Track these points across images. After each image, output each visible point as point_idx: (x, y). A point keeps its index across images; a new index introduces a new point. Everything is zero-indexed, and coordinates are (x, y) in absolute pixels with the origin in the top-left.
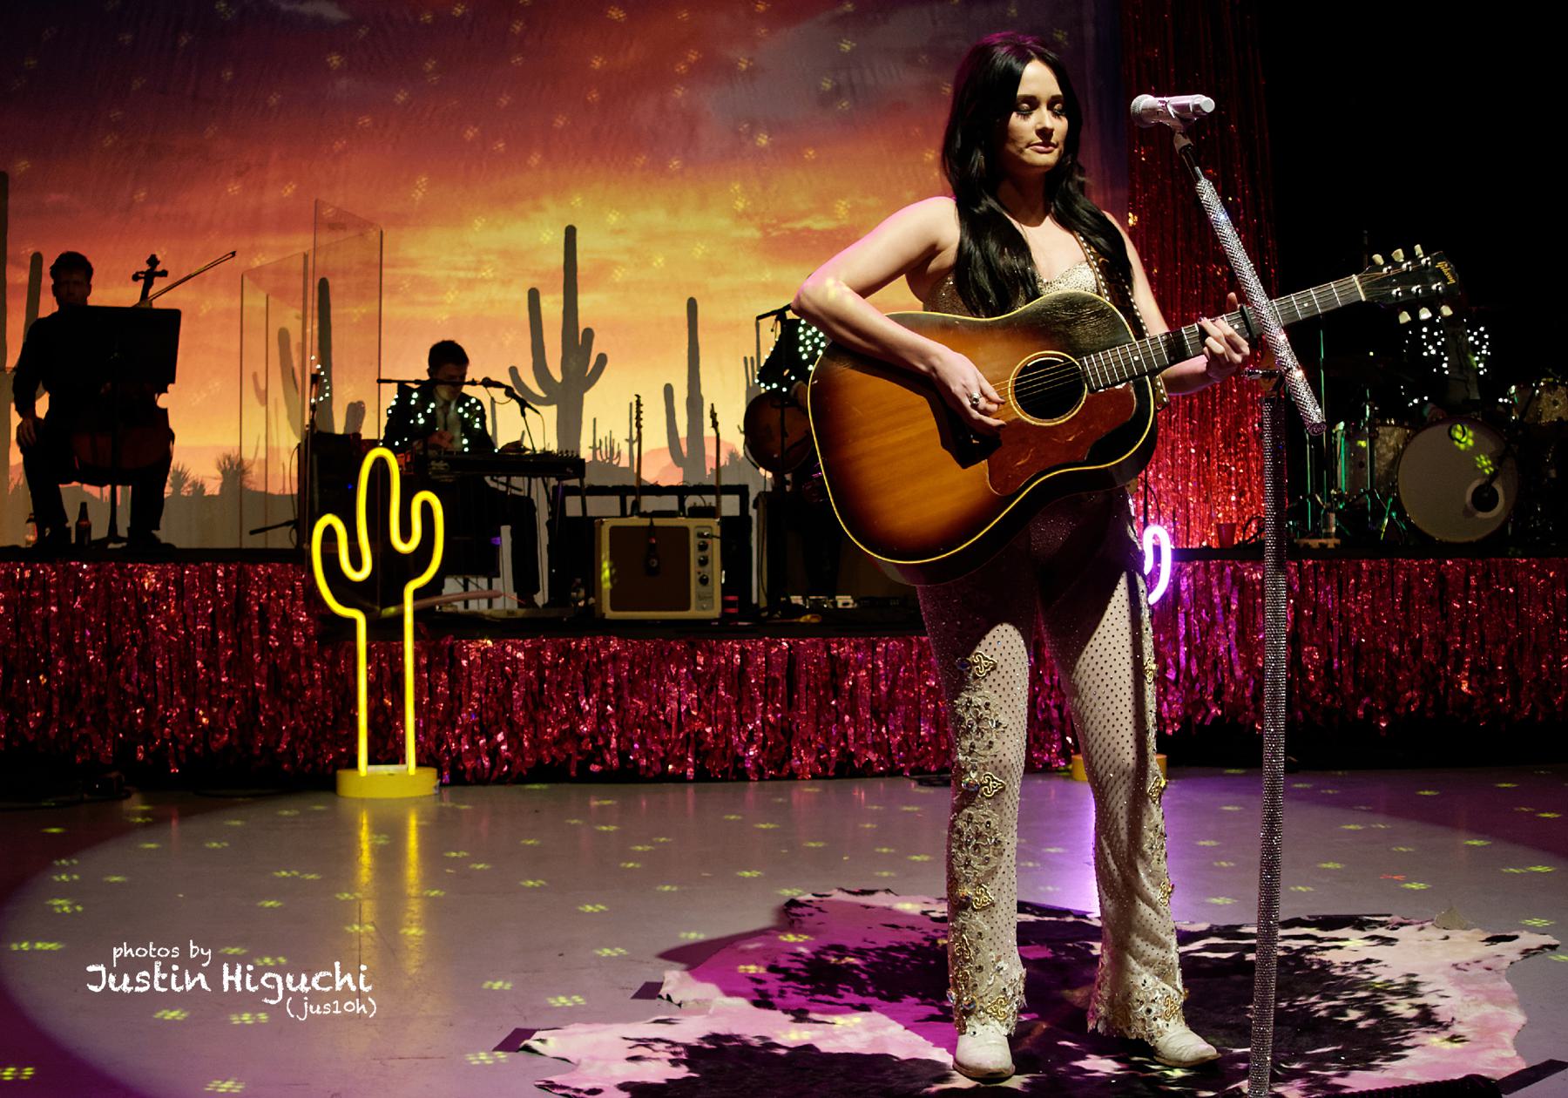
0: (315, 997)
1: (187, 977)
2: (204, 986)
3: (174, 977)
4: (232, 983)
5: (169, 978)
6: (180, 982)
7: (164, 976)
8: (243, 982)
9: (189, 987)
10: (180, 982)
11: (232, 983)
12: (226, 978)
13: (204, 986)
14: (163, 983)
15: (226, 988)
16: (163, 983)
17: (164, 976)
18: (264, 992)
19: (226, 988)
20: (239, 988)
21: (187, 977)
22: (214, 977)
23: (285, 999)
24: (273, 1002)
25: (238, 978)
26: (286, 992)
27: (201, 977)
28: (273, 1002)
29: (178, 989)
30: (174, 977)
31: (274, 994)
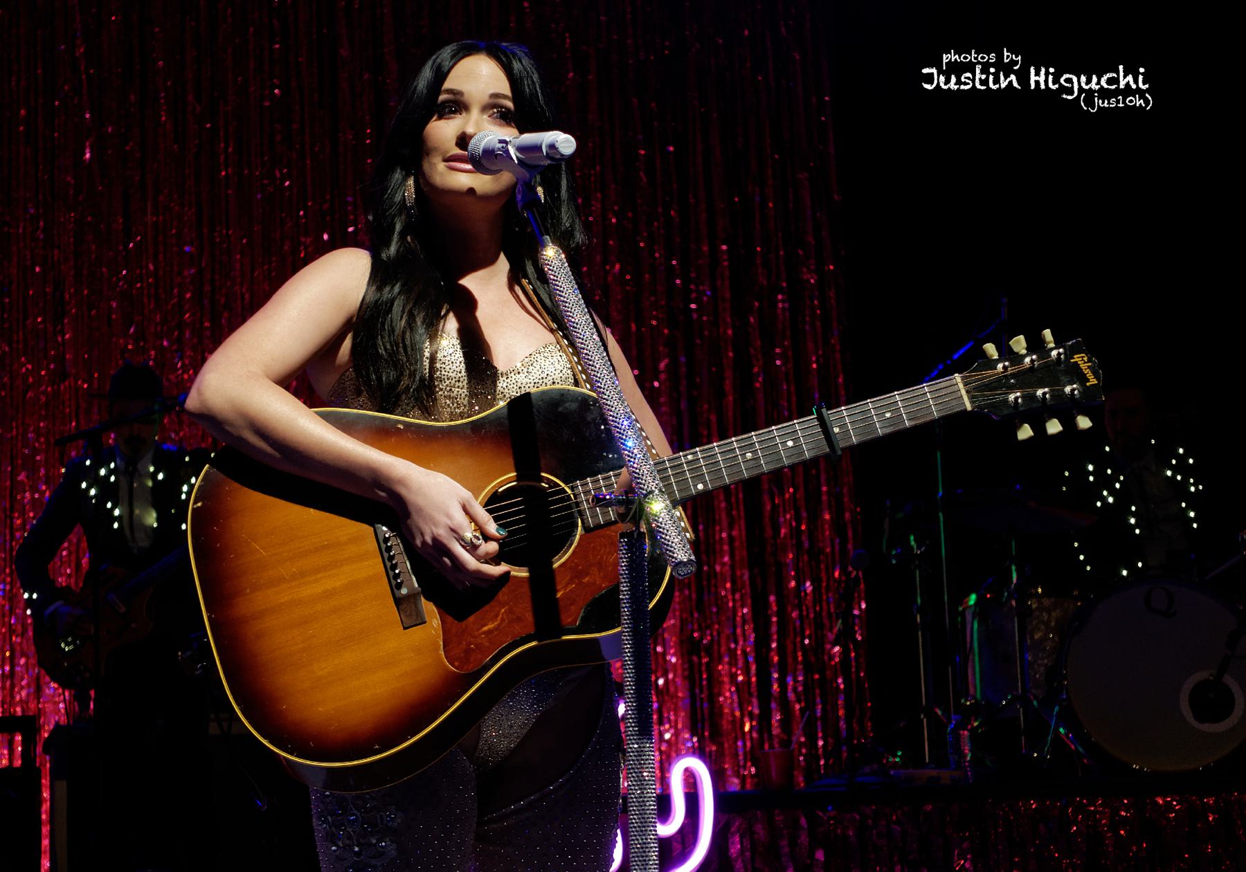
0: (1104, 94)
1: (1002, 78)
2: (1015, 84)
3: (991, 77)
4: (1037, 83)
5: (987, 79)
6: (996, 81)
7: (984, 77)
8: (1046, 82)
9: (1003, 86)
10: (996, 81)
11: (1037, 83)
12: (1033, 78)
13: (1015, 84)
14: (983, 82)
15: (1033, 87)
16: (983, 82)
17: (984, 77)
18: (1063, 90)
19: (1033, 87)
20: (1043, 87)
21: (1002, 78)
22: (1023, 77)
23: (1079, 95)
24: (1070, 97)
25: (1042, 79)
26: (1081, 89)
27: (1013, 77)
28: (1070, 97)
29: (994, 87)
30: (991, 77)
31: (1071, 91)
